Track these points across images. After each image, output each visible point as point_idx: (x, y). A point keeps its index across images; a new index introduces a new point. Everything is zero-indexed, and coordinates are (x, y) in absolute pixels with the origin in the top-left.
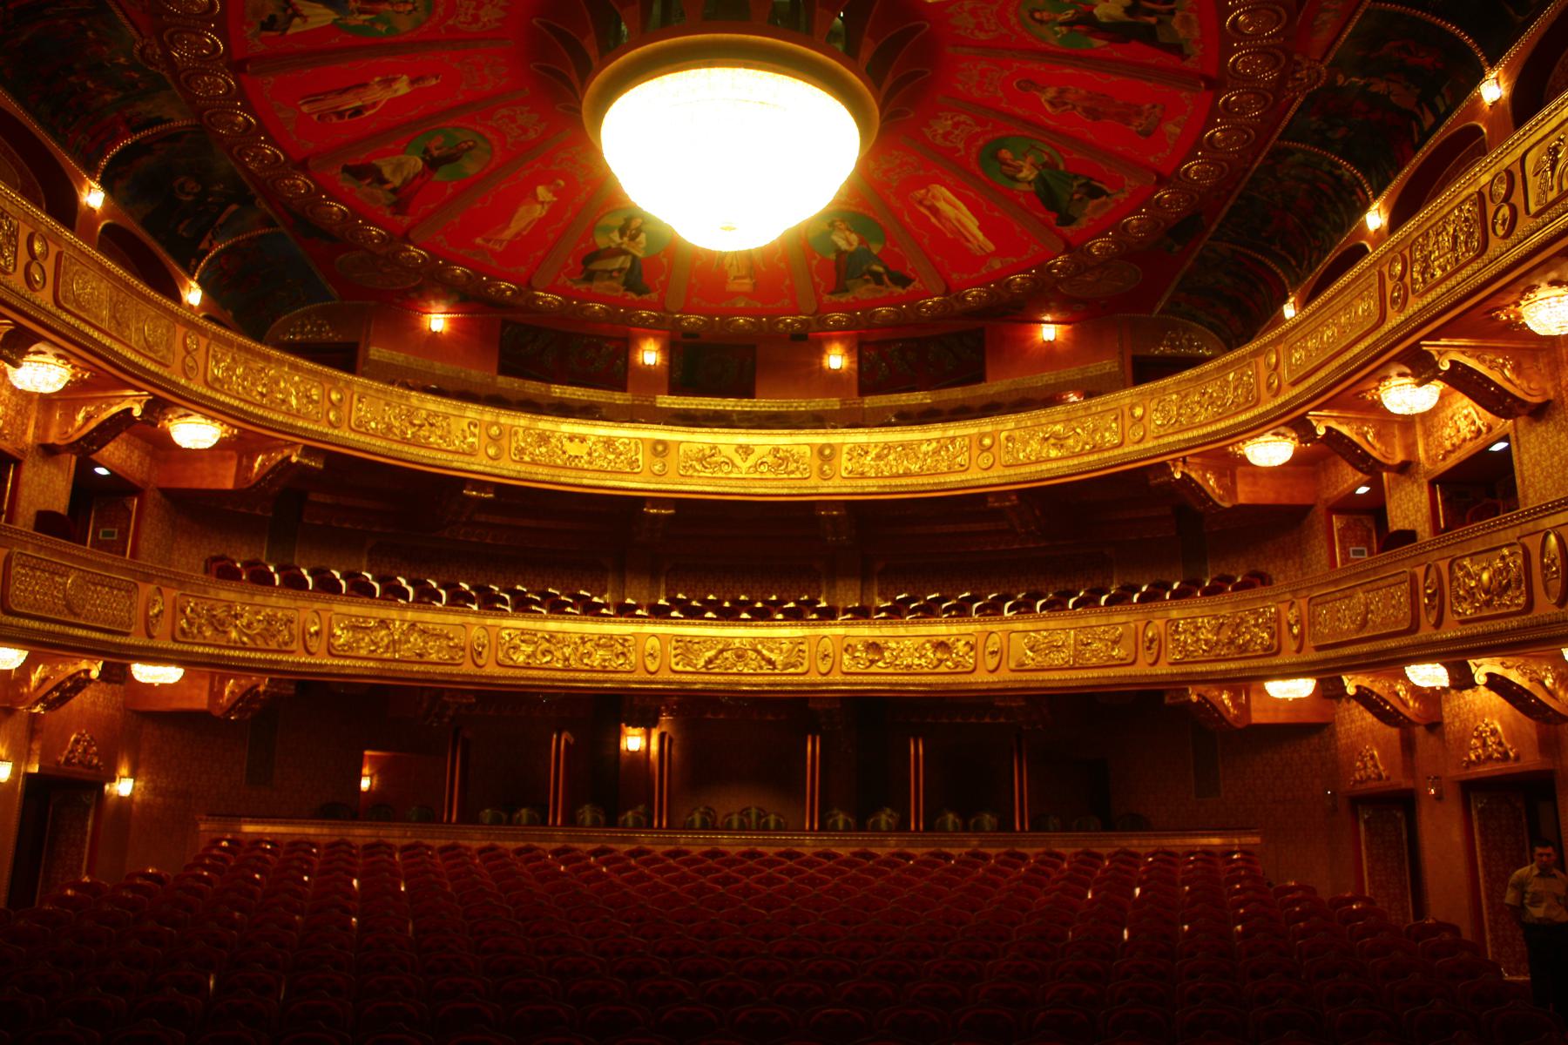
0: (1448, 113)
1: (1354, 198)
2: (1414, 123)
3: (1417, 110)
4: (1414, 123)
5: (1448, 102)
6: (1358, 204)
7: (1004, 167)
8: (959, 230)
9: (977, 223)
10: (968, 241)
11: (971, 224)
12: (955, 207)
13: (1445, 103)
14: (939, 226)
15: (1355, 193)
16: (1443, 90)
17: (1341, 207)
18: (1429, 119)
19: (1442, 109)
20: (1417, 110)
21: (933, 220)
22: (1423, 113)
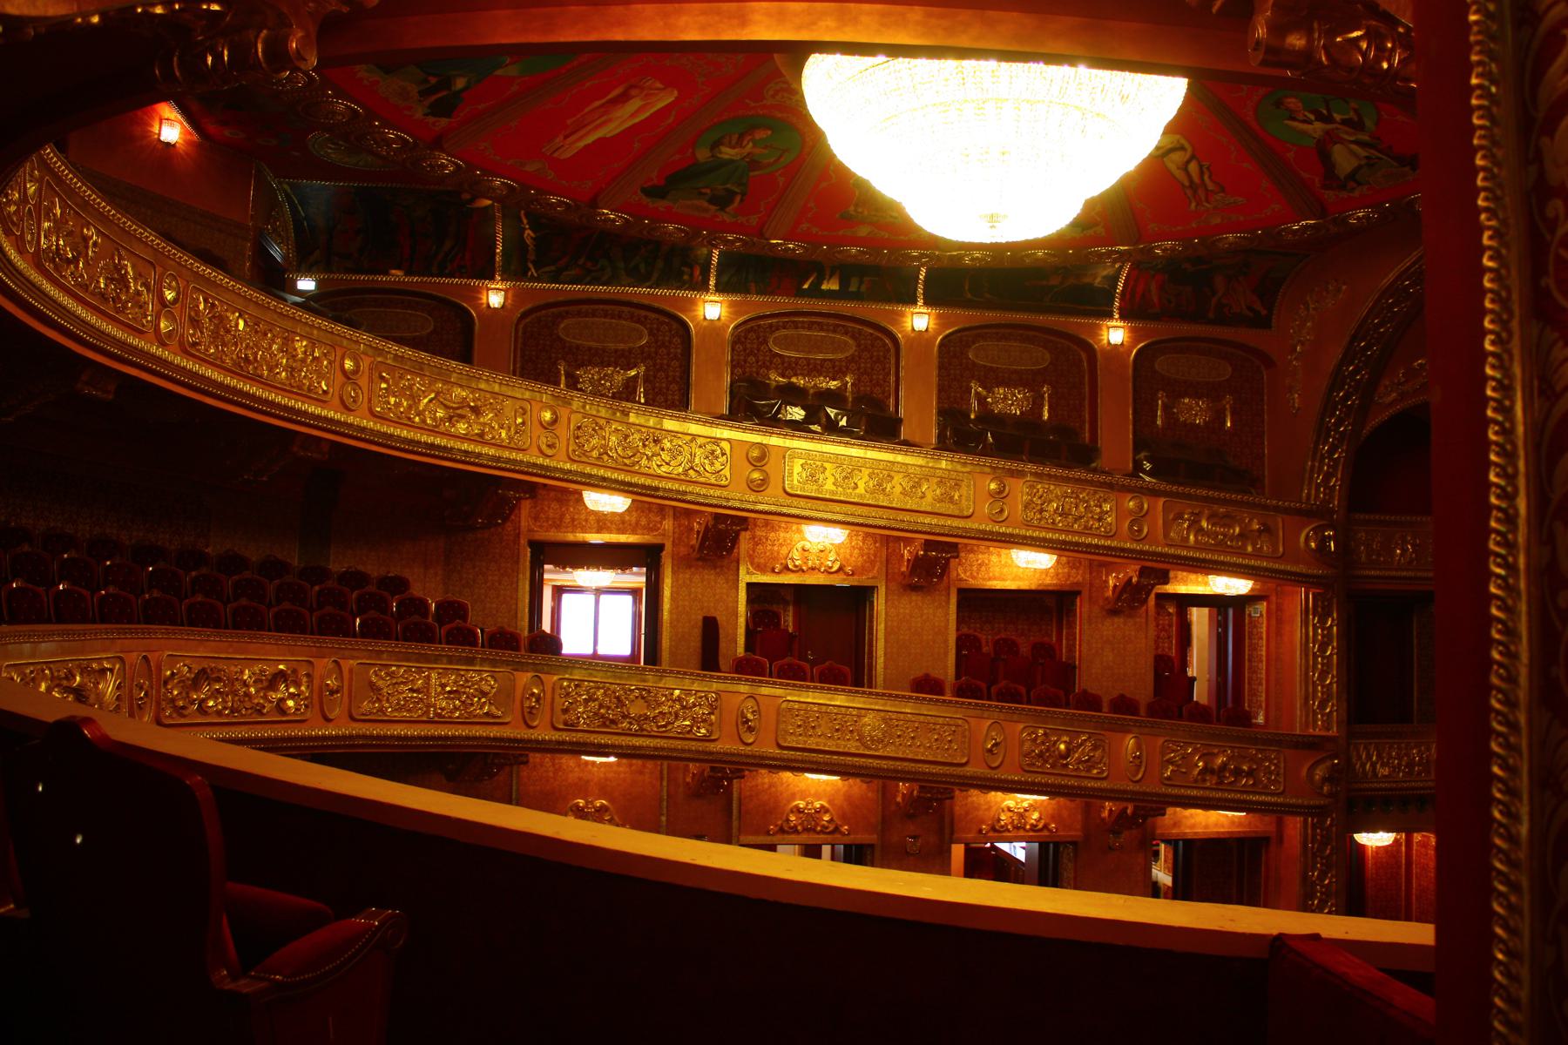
0: (857, 297)
1: (685, 269)
2: (815, 275)
3: (828, 273)
4: (815, 275)
5: (863, 288)
6: (686, 277)
7: (737, 136)
8: (586, 126)
9: (608, 136)
10: (566, 137)
11: (610, 129)
12: (633, 115)
13: (859, 288)
14: (587, 110)
15: (692, 268)
16: (866, 279)
17: (660, 264)
18: (832, 285)
19: (853, 288)
20: (828, 273)
21: (597, 103)
22: (831, 277)
